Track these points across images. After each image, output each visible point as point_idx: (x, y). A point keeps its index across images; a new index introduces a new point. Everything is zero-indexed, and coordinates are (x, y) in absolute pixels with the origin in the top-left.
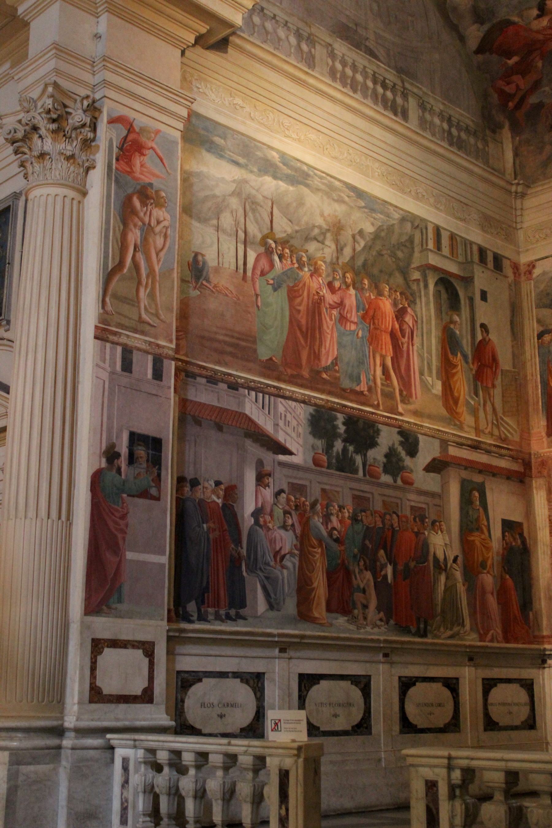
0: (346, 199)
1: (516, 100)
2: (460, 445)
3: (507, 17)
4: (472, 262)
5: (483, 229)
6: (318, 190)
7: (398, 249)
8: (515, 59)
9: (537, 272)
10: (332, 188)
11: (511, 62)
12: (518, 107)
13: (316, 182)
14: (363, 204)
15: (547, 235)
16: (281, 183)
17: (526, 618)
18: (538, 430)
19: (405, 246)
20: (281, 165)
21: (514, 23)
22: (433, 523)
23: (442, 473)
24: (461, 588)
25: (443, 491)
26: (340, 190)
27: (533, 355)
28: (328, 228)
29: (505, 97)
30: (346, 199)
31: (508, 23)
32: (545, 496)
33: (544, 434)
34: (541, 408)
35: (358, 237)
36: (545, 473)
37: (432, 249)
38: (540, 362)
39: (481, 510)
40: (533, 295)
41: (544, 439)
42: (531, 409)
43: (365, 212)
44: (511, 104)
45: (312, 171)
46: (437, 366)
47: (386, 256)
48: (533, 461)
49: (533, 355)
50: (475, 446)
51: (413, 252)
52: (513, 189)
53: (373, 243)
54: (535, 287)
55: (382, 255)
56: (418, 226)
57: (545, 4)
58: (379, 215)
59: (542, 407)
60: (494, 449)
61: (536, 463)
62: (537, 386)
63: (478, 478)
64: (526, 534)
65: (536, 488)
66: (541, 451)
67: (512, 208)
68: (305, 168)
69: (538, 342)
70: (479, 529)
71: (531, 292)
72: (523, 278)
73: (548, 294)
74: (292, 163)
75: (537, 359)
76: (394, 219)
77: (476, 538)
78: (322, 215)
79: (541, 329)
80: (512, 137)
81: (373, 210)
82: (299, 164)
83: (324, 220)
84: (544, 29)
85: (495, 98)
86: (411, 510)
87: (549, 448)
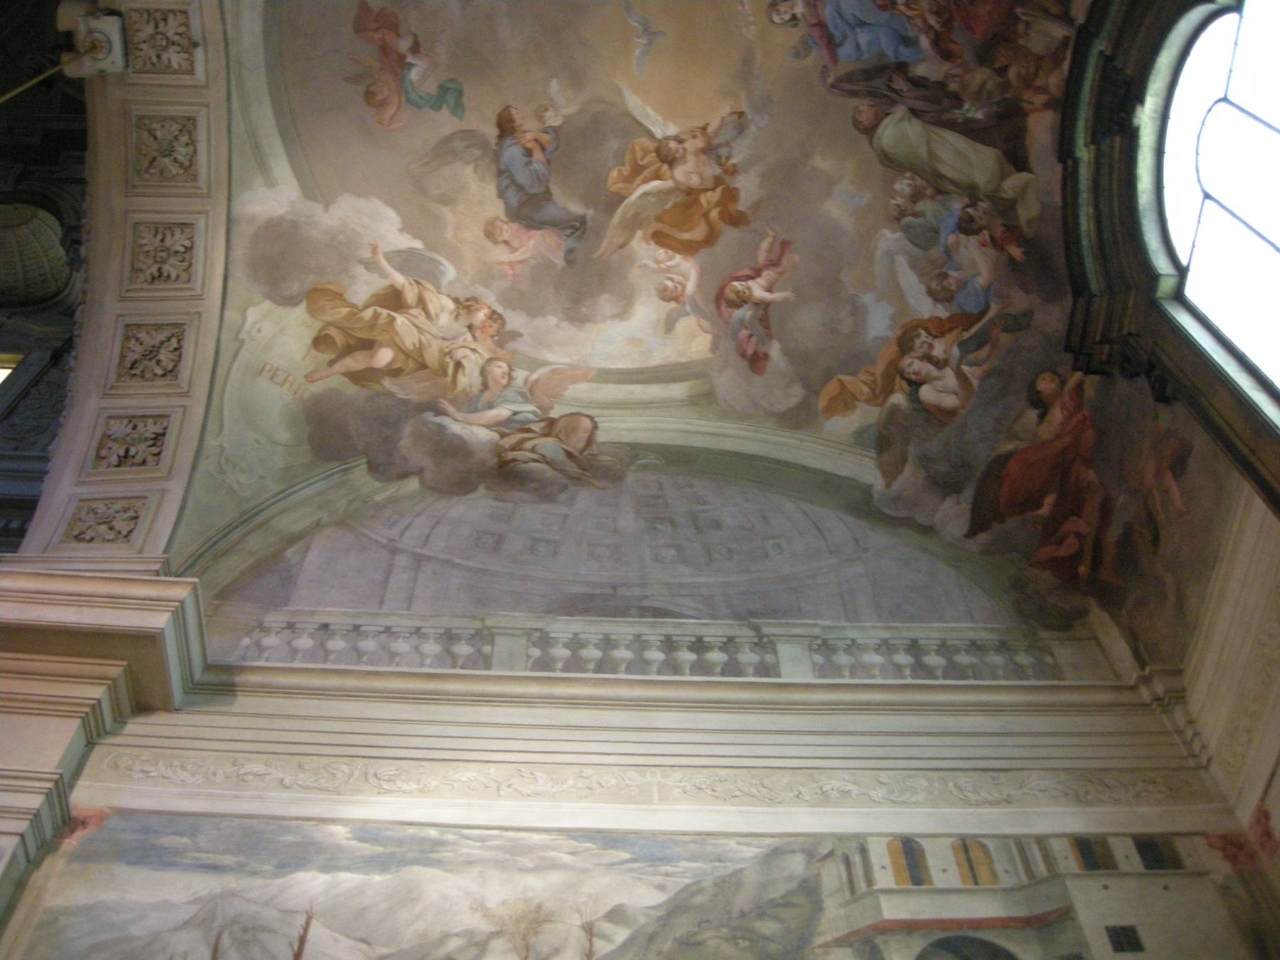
0: (567, 859)
1: (1088, 556)
3: (994, 454)
4: (1055, 875)
5: (1079, 799)
6: (469, 863)
7: (761, 916)
8: (1049, 500)
10: (516, 849)
11: (1045, 511)
12: (1096, 563)
13: (465, 850)
14: (625, 855)
16: (345, 875)
19: (787, 905)
20: (354, 843)
21: (1010, 455)
26: (547, 848)
28: (494, 929)
29: (1065, 569)
30: (567, 859)
31: (1003, 460)
35: (606, 927)
37: (892, 885)
43: (631, 870)
44: (1083, 570)
45: (455, 834)
47: (712, 944)
51: (818, 906)
53: (664, 925)
55: (699, 944)
56: (831, 854)
57: (1038, 392)
58: (684, 864)
67: (1167, 733)
68: (433, 833)
74: (389, 833)
76: (743, 860)
78: (479, 907)
80: (1113, 616)
81: (666, 860)
82: (411, 831)
83: (485, 916)
84: (1063, 424)
85: (1047, 578)
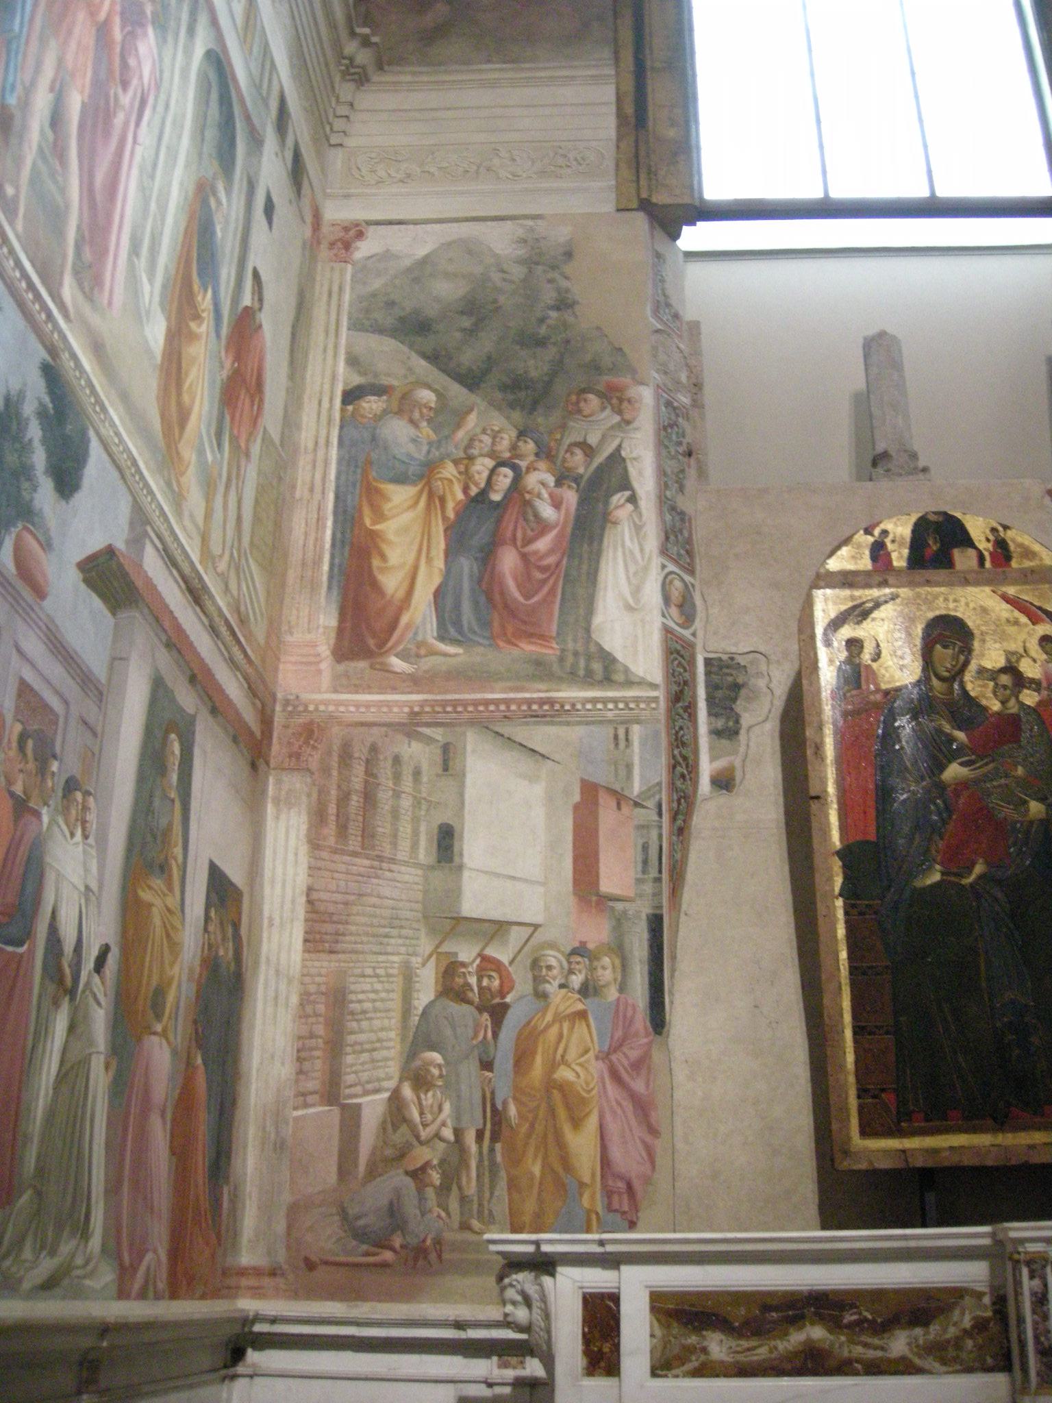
2: (171, 561)
9: (364, 249)
15: (409, 176)
17: (216, 1202)
18: (308, 637)
22: (71, 786)
23: (123, 615)
24: (100, 1078)
25: (109, 680)
27: (322, 441)
32: (304, 827)
33: (325, 650)
34: (325, 578)
36: (314, 761)
38: (340, 461)
39: (178, 805)
40: (347, 297)
41: (324, 666)
42: (292, 575)
46: (166, 267)
48: (279, 719)
49: (322, 441)
50: (196, 593)
52: (351, 47)
54: (354, 279)
59: (331, 578)
60: (223, 630)
61: (286, 727)
62: (320, 520)
63: (187, 699)
64: (243, 931)
65: (277, 801)
66: (305, 696)
69: (342, 410)
70: (164, 868)
71: (341, 289)
72: (324, 253)
73: (391, 304)
75: (334, 453)
77: (151, 894)
79: (357, 380)
86: (20, 694)
87: (336, 691)
